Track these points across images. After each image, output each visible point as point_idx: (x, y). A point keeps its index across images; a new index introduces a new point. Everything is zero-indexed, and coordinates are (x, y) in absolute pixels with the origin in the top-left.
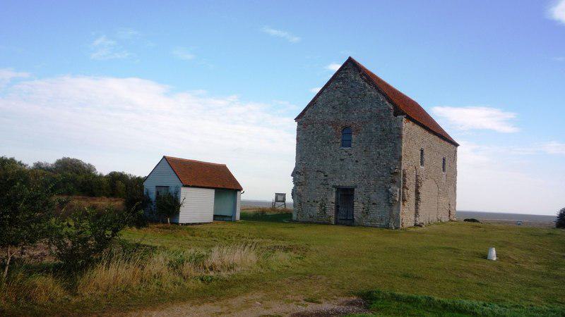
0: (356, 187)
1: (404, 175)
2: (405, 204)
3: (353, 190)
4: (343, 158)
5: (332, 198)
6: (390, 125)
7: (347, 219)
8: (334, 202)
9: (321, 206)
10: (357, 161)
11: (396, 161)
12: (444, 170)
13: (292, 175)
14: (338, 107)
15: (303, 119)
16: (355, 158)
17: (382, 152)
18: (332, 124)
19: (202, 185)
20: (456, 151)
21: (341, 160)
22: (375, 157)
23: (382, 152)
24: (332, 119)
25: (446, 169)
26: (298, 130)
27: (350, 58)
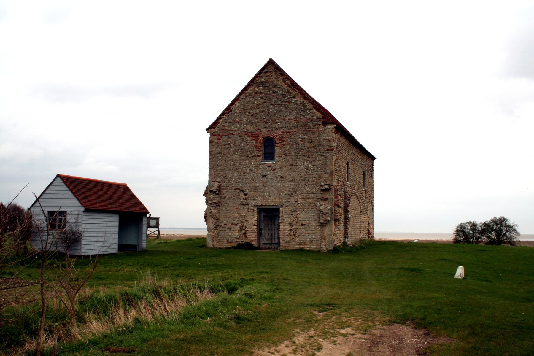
0: (282, 206)
2: (337, 223)
3: (278, 210)
4: (265, 173)
5: (254, 219)
6: (319, 136)
7: (272, 244)
8: (256, 224)
9: (241, 229)
10: (282, 177)
11: (326, 176)
13: (205, 195)
14: (258, 116)
15: (217, 129)
16: (279, 173)
17: (310, 166)
18: (254, 135)
19: (105, 208)
22: (303, 172)
23: (310, 166)
24: (251, 128)
25: (366, 185)
26: (211, 142)
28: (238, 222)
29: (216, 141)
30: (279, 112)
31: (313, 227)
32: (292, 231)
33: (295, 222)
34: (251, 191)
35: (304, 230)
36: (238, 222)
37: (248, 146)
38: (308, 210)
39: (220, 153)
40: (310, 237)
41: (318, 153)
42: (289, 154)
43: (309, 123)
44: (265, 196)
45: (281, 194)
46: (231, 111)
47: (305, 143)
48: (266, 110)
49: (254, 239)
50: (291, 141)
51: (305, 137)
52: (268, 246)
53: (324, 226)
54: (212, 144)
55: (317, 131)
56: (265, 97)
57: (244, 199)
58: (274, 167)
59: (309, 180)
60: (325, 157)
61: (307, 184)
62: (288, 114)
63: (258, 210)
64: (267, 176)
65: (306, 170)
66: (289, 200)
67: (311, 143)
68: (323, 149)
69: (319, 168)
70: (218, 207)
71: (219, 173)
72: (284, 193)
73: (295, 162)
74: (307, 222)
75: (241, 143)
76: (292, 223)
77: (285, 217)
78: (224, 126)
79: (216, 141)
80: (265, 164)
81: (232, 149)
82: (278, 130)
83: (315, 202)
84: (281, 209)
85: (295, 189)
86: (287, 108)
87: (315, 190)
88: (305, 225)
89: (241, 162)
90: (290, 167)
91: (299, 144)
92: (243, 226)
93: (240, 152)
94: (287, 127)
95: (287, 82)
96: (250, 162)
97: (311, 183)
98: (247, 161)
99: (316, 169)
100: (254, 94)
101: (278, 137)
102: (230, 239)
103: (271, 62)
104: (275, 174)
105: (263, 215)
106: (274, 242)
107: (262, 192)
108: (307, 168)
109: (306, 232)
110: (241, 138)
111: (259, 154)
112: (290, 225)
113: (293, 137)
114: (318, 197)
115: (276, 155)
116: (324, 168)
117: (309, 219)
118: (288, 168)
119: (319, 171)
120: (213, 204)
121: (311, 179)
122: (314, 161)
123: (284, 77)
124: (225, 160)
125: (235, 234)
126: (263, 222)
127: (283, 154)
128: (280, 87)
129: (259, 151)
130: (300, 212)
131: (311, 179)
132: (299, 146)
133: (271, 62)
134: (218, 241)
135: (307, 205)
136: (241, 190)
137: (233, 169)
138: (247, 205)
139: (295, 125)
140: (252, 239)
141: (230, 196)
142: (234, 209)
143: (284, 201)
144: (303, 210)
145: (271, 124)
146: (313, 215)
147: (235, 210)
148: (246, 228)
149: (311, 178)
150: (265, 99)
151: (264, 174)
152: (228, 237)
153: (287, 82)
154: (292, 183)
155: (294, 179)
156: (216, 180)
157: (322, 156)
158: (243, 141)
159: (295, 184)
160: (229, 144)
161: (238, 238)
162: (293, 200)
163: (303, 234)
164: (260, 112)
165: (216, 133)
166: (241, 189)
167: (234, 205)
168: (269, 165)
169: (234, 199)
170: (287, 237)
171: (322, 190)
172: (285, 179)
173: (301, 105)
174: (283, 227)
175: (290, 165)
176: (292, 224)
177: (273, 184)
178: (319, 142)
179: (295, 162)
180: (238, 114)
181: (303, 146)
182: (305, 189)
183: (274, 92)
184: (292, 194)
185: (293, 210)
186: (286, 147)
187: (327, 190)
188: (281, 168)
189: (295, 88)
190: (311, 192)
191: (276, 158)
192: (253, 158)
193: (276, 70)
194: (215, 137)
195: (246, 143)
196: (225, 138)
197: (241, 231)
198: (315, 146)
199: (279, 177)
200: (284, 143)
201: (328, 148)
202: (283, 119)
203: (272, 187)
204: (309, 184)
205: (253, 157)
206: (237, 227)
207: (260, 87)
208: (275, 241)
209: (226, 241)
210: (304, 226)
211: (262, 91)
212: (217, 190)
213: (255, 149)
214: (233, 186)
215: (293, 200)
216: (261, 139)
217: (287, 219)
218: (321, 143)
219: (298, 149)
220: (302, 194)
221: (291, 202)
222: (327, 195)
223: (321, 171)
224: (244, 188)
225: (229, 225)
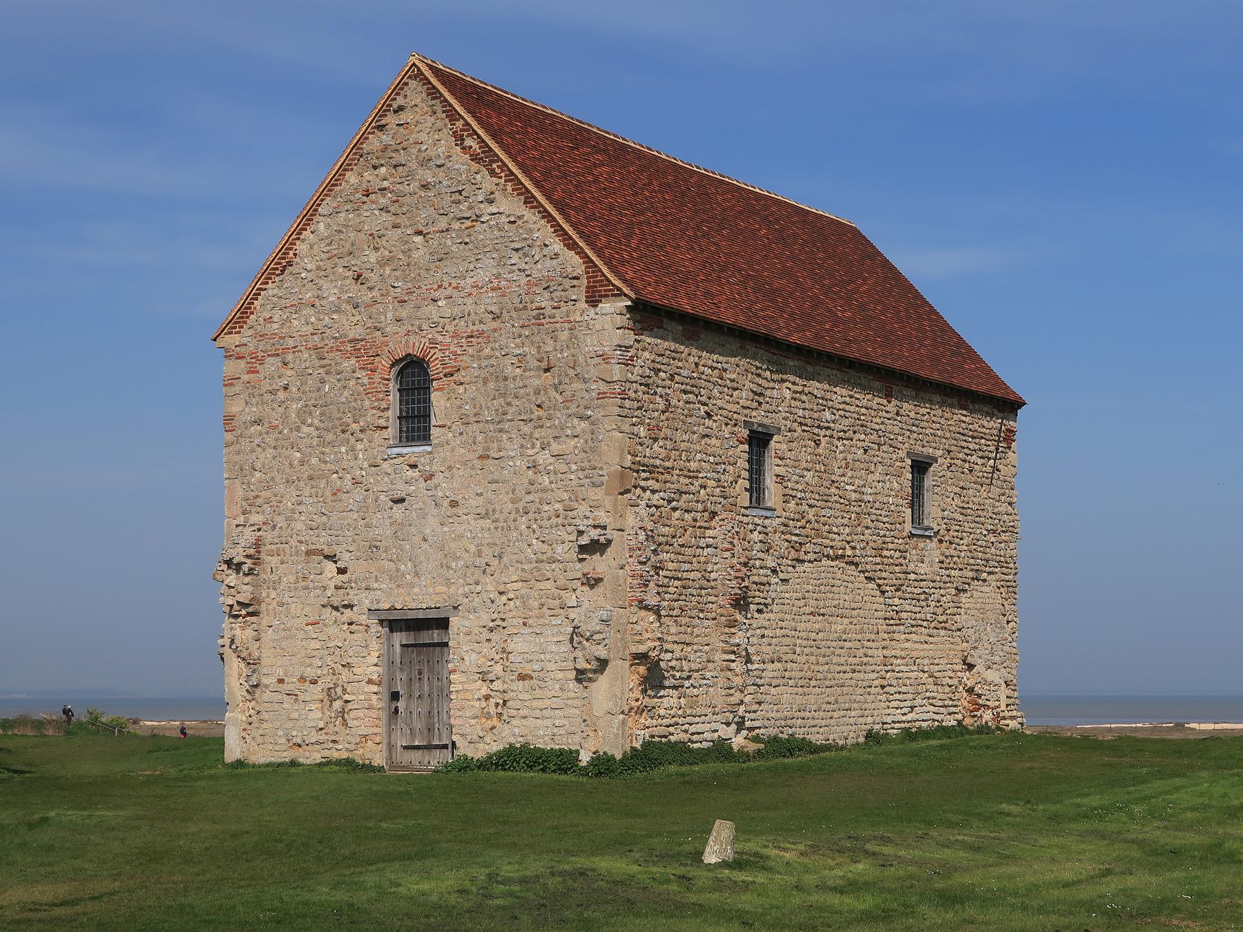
3: (442, 624)
4: (401, 490)
9: (331, 698)
10: (454, 504)
14: (373, 278)
23: (544, 458)
24: (352, 326)
28: (319, 672)
29: (246, 377)
30: (443, 257)
31: (557, 686)
32: (492, 701)
33: (498, 669)
35: (528, 697)
36: (319, 672)
37: (346, 393)
38: (541, 621)
39: (257, 422)
40: (548, 722)
41: (568, 408)
42: (476, 415)
43: (538, 298)
45: (453, 565)
46: (290, 264)
47: (527, 373)
48: (401, 256)
49: (371, 731)
51: (526, 349)
54: (233, 389)
55: (566, 325)
56: (396, 205)
57: (337, 588)
58: (428, 468)
59: (538, 511)
60: (593, 423)
61: (535, 526)
62: (472, 267)
64: (407, 502)
65: (530, 472)
66: (479, 588)
67: (547, 370)
69: (574, 467)
70: (254, 619)
72: (461, 563)
73: (495, 445)
75: (323, 382)
76: (489, 672)
78: (269, 320)
79: (246, 377)
80: (401, 455)
81: (294, 406)
84: (454, 621)
85: (496, 544)
87: (559, 549)
89: (323, 453)
91: (506, 379)
92: (336, 685)
95: (469, 142)
97: (545, 523)
98: (343, 449)
99: (563, 468)
100: (359, 195)
101: (439, 355)
102: (295, 733)
104: (430, 493)
105: (403, 646)
106: (436, 742)
108: (533, 466)
109: (535, 704)
110: (323, 362)
111: (382, 422)
113: (487, 351)
114: (570, 575)
115: (433, 422)
116: (586, 464)
117: (542, 657)
118: (473, 468)
119: (573, 477)
124: (275, 448)
125: (311, 716)
127: (455, 417)
130: (516, 631)
131: (547, 508)
132: (506, 387)
134: (260, 739)
135: (536, 604)
139: (493, 308)
141: (292, 578)
143: (461, 591)
144: (525, 624)
146: (555, 639)
148: (344, 690)
151: (399, 495)
152: (290, 725)
153: (469, 142)
156: (246, 520)
157: (582, 418)
161: (321, 729)
162: (490, 588)
164: (383, 263)
165: (243, 349)
166: (327, 552)
167: (308, 610)
168: (413, 460)
169: (307, 588)
170: (473, 721)
171: (582, 549)
172: (465, 511)
174: (460, 687)
175: (481, 457)
177: (428, 531)
179: (495, 445)
180: (310, 276)
181: (521, 384)
183: (425, 187)
185: (491, 624)
187: (596, 547)
188: (450, 468)
189: (494, 166)
190: (550, 554)
191: (434, 432)
192: (362, 436)
193: (433, 99)
194: (242, 363)
196: (272, 364)
197: (331, 706)
198: (560, 383)
199: (446, 503)
201: (603, 387)
202: (454, 285)
203: (425, 540)
204: (541, 527)
206: (316, 691)
208: (440, 740)
209: (283, 740)
211: (386, 184)
212: (248, 556)
213: (367, 402)
214: (301, 542)
216: (385, 362)
217: (474, 656)
218: (579, 370)
219: (503, 395)
221: (484, 595)
222: (598, 564)
223: (581, 474)
224: (337, 549)
225: (292, 684)
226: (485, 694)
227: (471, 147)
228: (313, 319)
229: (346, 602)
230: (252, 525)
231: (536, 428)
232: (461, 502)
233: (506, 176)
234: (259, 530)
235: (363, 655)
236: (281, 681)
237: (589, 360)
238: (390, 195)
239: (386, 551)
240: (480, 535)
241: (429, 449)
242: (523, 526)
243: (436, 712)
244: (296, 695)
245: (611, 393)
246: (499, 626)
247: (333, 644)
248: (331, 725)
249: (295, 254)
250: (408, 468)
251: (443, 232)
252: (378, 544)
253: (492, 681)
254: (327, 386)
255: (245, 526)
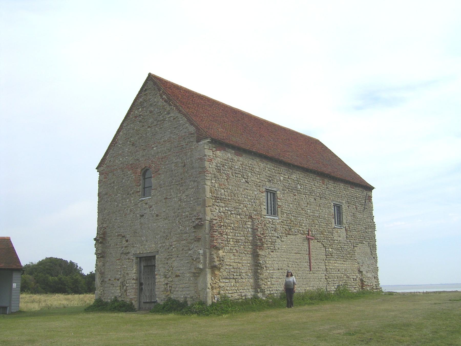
1: (211, 227)
2: (217, 272)
5: (133, 272)
9: (123, 284)
11: (199, 208)
12: (340, 222)
20: (370, 198)
21: (142, 216)
23: (184, 197)
27: (150, 75)
32: (169, 285)
34: (131, 237)
36: (120, 276)
40: (184, 293)
41: (190, 178)
42: (164, 184)
43: (182, 142)
44: (143, 241)
46: (116, 143)
47: (178, 168)
50: (165, 168)
51: (178, 160)
52: (148, 305)
53: (198, 276)
55: (189, 150)
59: (182, 215)
61: (180, 221)
63: (138, 259)
66: (164, 244)
68: (195, 173)
71: (105, 218)
74: (182, 272)
75: (123, 179)
76: (167, 275)
77: (160, 267)
79: (104, 180)
80: (142, 200)
82: (154, 157)
83: (189, 244)
85: (169, 228)
86: (162, 128)
88: (179, 276)
90: (164, 201)
91: (172, 171)
93: (122, 189)
94: (162, 151)
95: (164, 96)
96: (130, 200)
97: (184, 220)
103: (151, 79)
105: (144, 266)
106: (153, 301)
107: (140, 237)
108: (180, 200)
109: (181, 286)
111: (138, 190)
112: (166, 277)
113: (167, 162)
119: (192, 202)
120: (98, 254)
121: (184, 214)
122: (187, 189)
123: (161, 92)
126: (143, 275)
128: (156, 104)
129: (137, 186)
131: (184, 214)
133: (151, 79)
135: (181, 249)
136: (123, 237)
137: (116, 211)
138: (128, 255)
139: (169, 148)
140: (131, 297)
141: (113, 245)
142: (117, 260)
144: (177, 257)
145: (148, 151)
147: (118, 261)
149: (184, 213)
150: (143, 122)
154: (167, 221)
155: (169, 216)
156: (102, 226)
157: (194, 181)
158: (124, 176)
159: (169, 223)
160: (114, 182)
161: (120, 296)
162: (167, 244)
163: (177, 289)
166: (123, 235)
173: (175, 120)
176: (168, 276)
178: (191, 165)
182: (179, 228)
183: (151, 112)
184: (167, 236)
186: (161, 176)
195: (127, 178)
197: (123, 288)
200: (160, 172)
203: (149, 229)
205: (133, 193)
207: (139, 109)
208: (154, 300)
210: (178, 278)
212: (100, 238)
215: (167, 244)
220: (177, 235)
221: (166, 247)
226: (166, 283)
227: (164, 98)
228: (121, 159)
229: (127, 252)
230: (103, 228)
231: (181, 186)
232: (159, 214)
233: (174, 105)
234: (105, 229)
235: (131, 270)
236: (110, 280)
237: (196, 161)
238: (142, 117)
239: (138, 234)
240: (164, 226)
241: (150, 197)
242: (177, 221)
243: (153, 290)
244: (113, 284)
245: (203, 172)
246: (170, 258)
247: (124, 266)
248: (123, 295)
249: (118, 140)
250: (145, 204)
251: (155, 125)
252: (136, 231)
253: (168, 278)
254: (124, 180)
255: (102, 228)
